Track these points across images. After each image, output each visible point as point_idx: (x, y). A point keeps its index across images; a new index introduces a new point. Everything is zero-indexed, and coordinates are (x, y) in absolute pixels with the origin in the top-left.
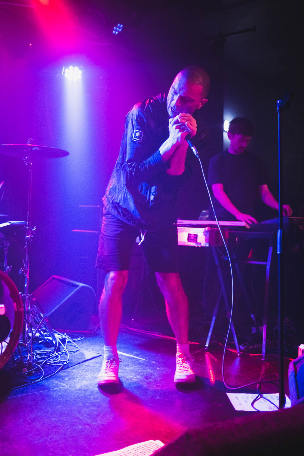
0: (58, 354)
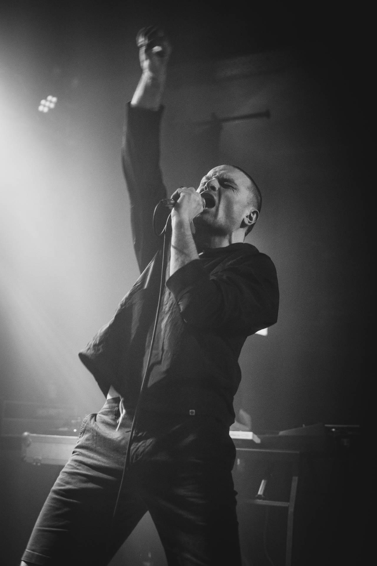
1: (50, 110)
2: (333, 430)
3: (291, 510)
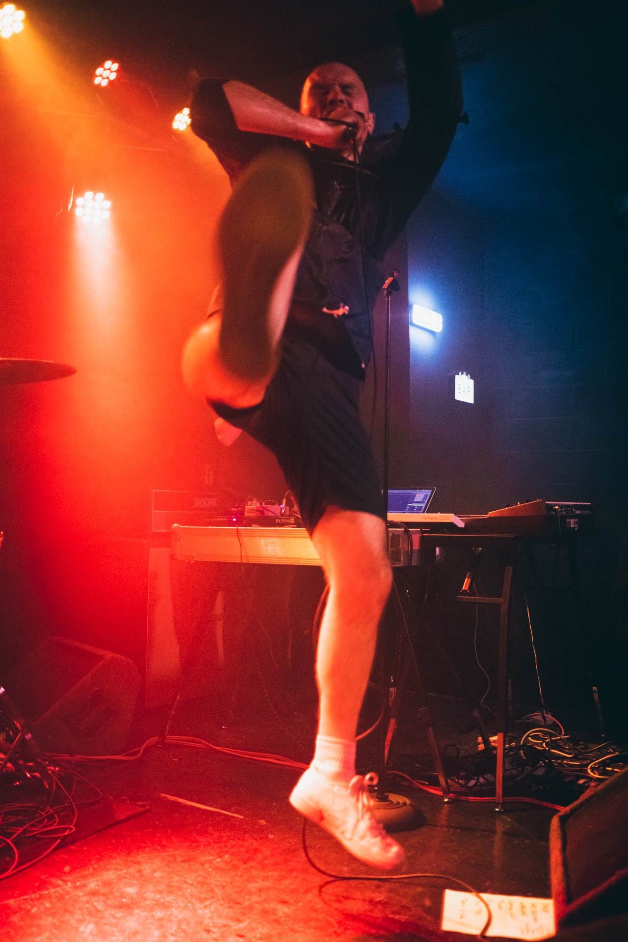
0: (53, 810)
1: (111, 83)
2: (557, 507)
3: (504, 609)
